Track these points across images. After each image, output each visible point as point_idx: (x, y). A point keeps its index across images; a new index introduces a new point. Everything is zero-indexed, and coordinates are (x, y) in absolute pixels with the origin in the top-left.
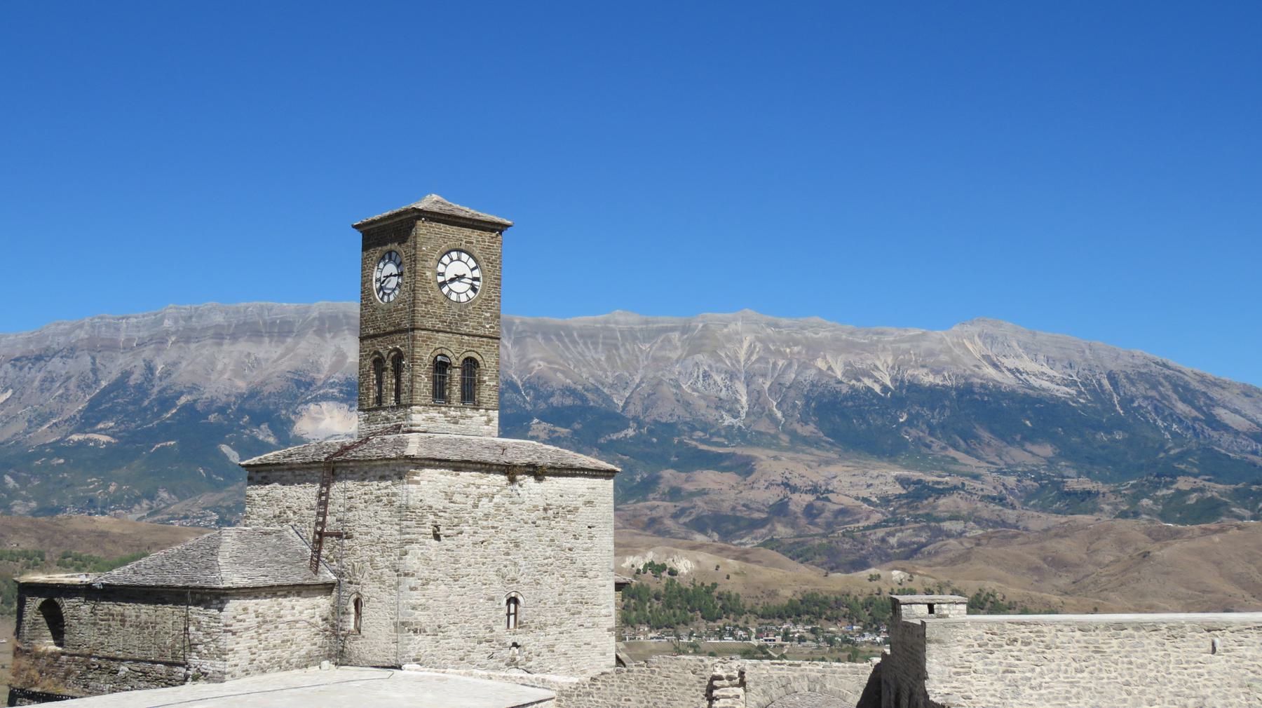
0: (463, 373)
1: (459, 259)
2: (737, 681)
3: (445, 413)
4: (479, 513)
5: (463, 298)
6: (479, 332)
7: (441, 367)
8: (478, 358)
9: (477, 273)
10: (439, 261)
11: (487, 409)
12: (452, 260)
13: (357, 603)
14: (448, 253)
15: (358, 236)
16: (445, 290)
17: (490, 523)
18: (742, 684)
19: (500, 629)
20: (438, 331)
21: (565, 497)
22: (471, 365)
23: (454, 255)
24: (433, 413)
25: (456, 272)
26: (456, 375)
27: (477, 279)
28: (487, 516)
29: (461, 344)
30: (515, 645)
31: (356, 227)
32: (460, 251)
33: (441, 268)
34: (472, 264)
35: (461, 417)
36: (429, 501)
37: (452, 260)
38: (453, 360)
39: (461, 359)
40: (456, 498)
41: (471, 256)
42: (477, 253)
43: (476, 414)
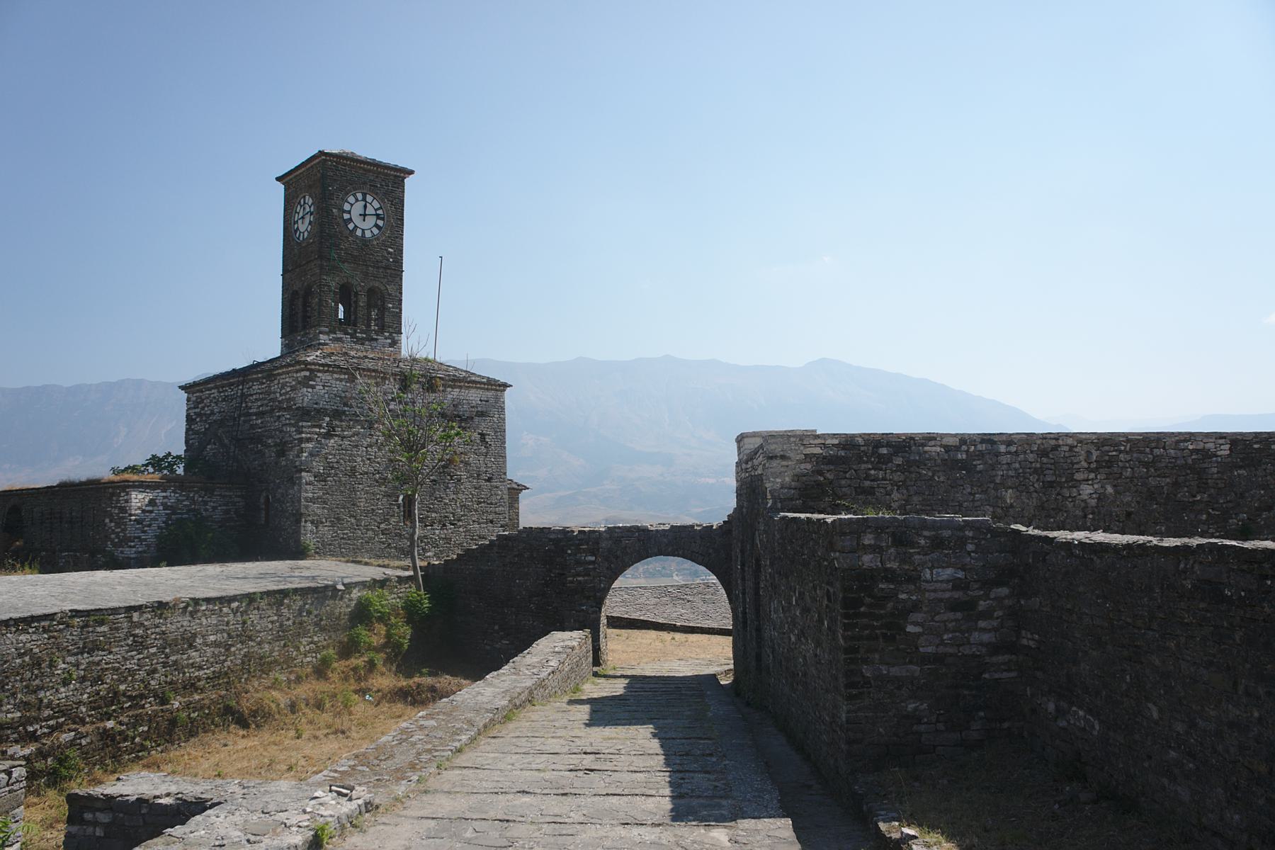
12: (357, 200)
15: (281, 187)
16: (351, 226)
29: (366, 274)
31: (278, 179)
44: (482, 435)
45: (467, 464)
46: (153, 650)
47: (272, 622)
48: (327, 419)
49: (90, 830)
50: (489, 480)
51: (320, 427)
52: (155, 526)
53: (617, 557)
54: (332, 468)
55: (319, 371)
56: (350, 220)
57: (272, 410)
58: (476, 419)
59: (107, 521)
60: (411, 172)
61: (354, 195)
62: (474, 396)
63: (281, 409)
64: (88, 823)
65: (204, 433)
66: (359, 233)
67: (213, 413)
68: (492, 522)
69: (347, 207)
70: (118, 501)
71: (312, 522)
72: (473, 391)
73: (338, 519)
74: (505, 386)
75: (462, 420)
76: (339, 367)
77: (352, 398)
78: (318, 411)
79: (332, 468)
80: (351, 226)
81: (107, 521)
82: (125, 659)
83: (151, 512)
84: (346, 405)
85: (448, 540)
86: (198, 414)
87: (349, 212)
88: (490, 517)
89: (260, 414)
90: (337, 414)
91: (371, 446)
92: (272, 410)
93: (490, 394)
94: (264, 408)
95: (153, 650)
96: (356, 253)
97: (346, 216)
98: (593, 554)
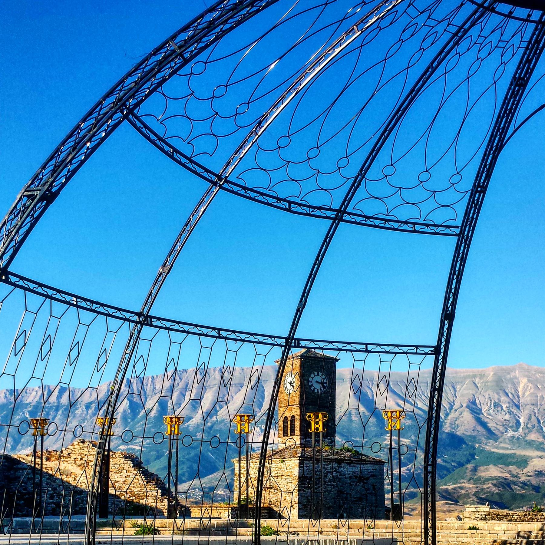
1: (318, 375)
9: (325, 381)
12: (315, 376)
16: (312, 388)
17: (332, 483)
27: (326, 383)
51: (305, 484)
56: (312, 385)
58: (371, 478)
60: (340, 359)
61: (314, 373)
62: (369, 468)
69: (310, 379)
72: (368, 465)
75: (365, 479)
80: (312, 388)
87: (311, 382)
93: (377, 466)
97: (310, 384)
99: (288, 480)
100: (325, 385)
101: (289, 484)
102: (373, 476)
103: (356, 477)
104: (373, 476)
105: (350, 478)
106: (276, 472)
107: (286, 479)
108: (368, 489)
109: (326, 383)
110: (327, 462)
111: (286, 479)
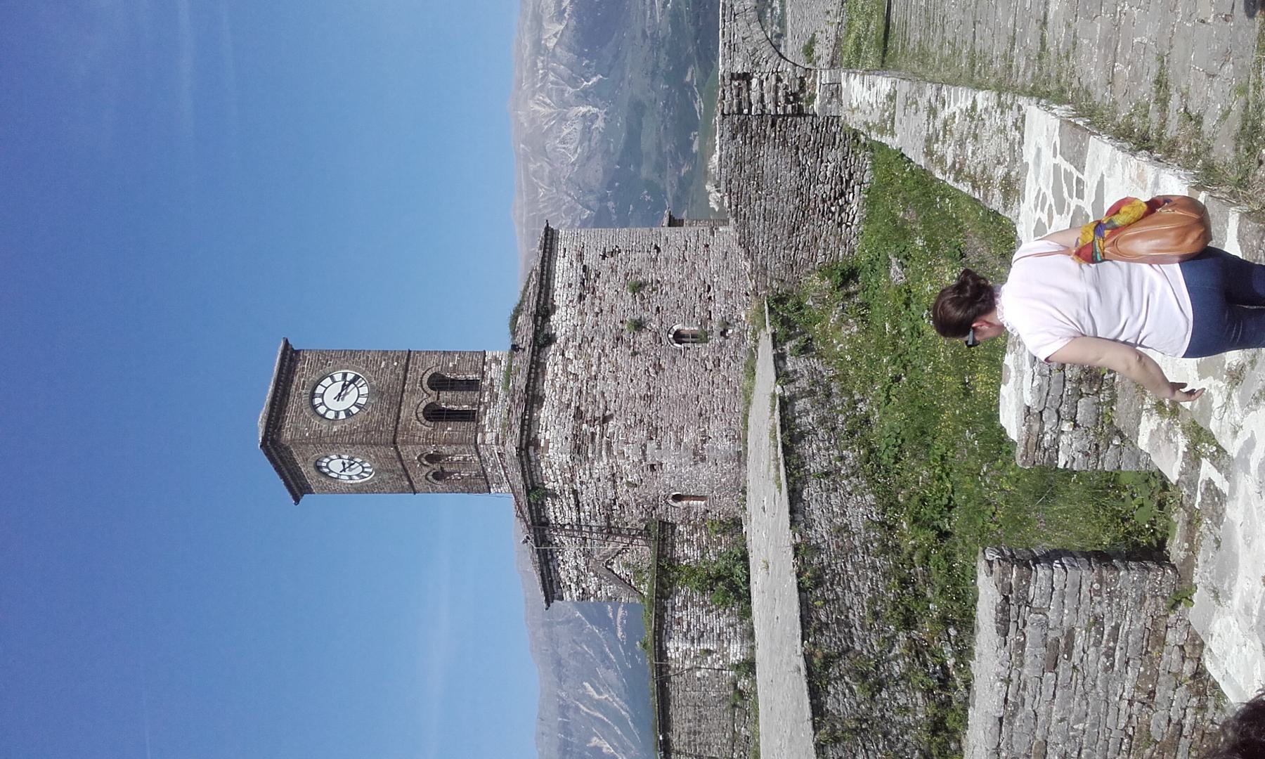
0: (445, 389)
1: (322, 396)
2: (744, 84)
3: (486, 408)
4: (583, 375)
5: (364, 390)
6: (401, 372)
7: (435, 414)
8: (429, 373)
9: (338, 377)
10: (323, 416)
11: (484, 363)
12: (323, 404)
13: (677, 498)
14: (315, 408)
16: (355, 410)
17: (594, 360)
18: (746, 77)
19: (704, 351)
20: (399, 417)
21: (572, 281)
22: (439, 383)
23: (317, 401)
24: (486, 421)
25: (338, 398)
26: (446, 395)
27: (345, 375)
28: (588, 367)
30: (723, 334)
31: (297, 500)
32: (313, 395)
33: (330, 415)
34: (327, 381)
35: (491, 391)
36: (568, 431)
37: (323, 404)
38: (430, 400)
39: (430, 391)
40: (564, 400)
41: (318, 383)
42: (316, 377)
43: (490, 374)
44: (604, 257)
45: (639, 272)
46: (849, 567)
47: (819, 449)
48: (585, 426)
49: (1064, 439)
50: (658, 250)
51: (593, 434)
52: (705, 619)
53: (756, 50)
54: (641, 421)
55: (529, 435)
57: (575, 492)
59: (698, 674)
63: (572, 481)
64: (1056, 442)
65: (601, 578)
66: (362, 401)
67: (577, 568)
68: (707, 246)
70: (676, 660)
71: (704, 442)
73: (701, 415)
74: (547, 228)
76: (524, 414)
77: (560, 399)
78: (575, 436)
79: (641, 421)
80: (355, 410)
81: (698, 674)
82: (858, 594)
83: (689, 624)
84: (569, 406)
85: (728, 294)
86: (577, 584)
88: (702, 248)
89: (577, 505)
90: (579, 415)
91: (616, 378)
92: (575, 492)
94: (572, 501)
95: (849, 567)
96: (385, 405)
97: (342, 416)
98: (749, 84)
99: (585, 478)
100: (350, 377)
101: (595, 476)
102: (581, 256)
103: (581, 298)
104: (581, 256)
105: (581, 313)
106: (566, 508)
107: (582, 483)
108: (614, 270)
109: (345, 375)
110: (537, 374)
111: (582, 483)
